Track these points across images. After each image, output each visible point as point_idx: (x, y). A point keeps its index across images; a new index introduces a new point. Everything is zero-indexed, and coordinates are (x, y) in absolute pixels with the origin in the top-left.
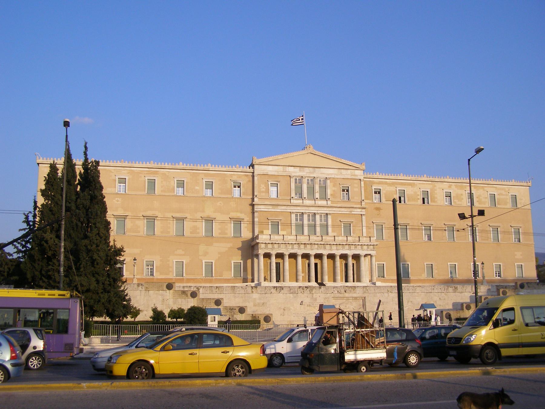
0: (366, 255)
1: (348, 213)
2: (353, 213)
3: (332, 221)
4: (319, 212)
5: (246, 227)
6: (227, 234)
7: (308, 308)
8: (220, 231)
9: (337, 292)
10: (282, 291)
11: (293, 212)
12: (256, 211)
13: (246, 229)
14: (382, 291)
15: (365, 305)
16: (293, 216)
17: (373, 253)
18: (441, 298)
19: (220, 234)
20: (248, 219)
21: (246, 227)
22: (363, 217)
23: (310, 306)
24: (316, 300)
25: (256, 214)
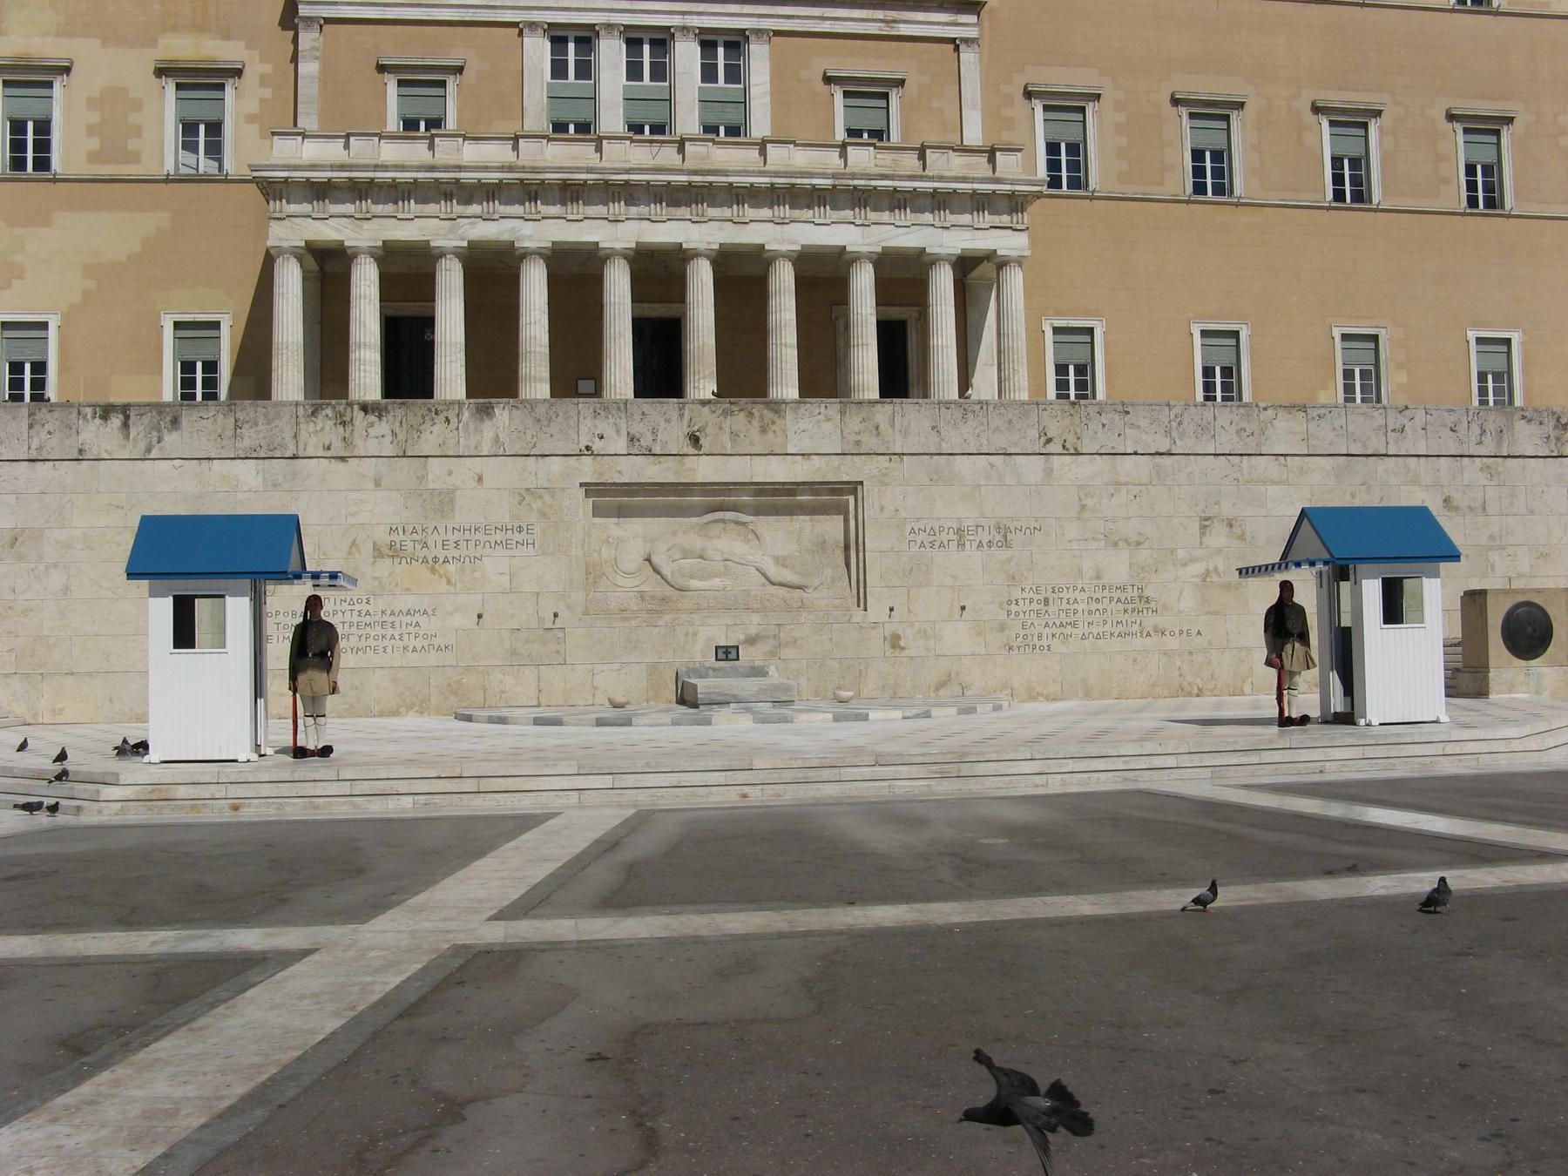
0: (965, 265)
1: (873, 29)
2: (905, 30)
3: (777, 75)
4: (696, 22)
5: (251, 119)
6: (135, 158)
7: (384, 568)
8: (94, 144)
9: (621, 445)
10: (172, 439)
11: (533, 25)
12: (310, 20)
13: (255, 128)
14: (1000, 442)
15: (861, 547)
16: (538, 51)
17: (1009, 243)
18: (1459, 498)
19: (93, 158)
20: (267, 68)
21: (251, 119)
22: (968, 56)
23: (395, 551)
24: (444, 502)
25: (308, 38)
